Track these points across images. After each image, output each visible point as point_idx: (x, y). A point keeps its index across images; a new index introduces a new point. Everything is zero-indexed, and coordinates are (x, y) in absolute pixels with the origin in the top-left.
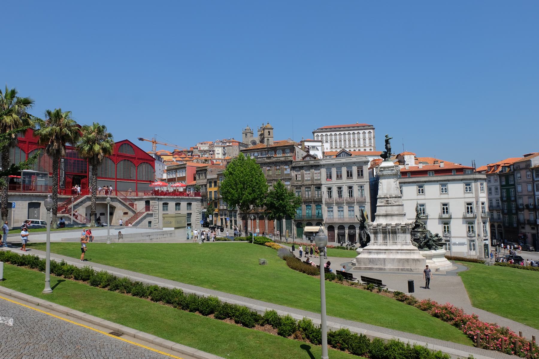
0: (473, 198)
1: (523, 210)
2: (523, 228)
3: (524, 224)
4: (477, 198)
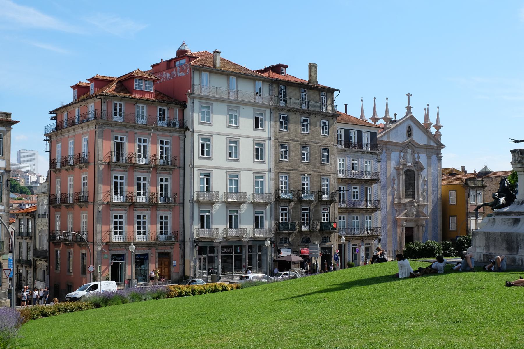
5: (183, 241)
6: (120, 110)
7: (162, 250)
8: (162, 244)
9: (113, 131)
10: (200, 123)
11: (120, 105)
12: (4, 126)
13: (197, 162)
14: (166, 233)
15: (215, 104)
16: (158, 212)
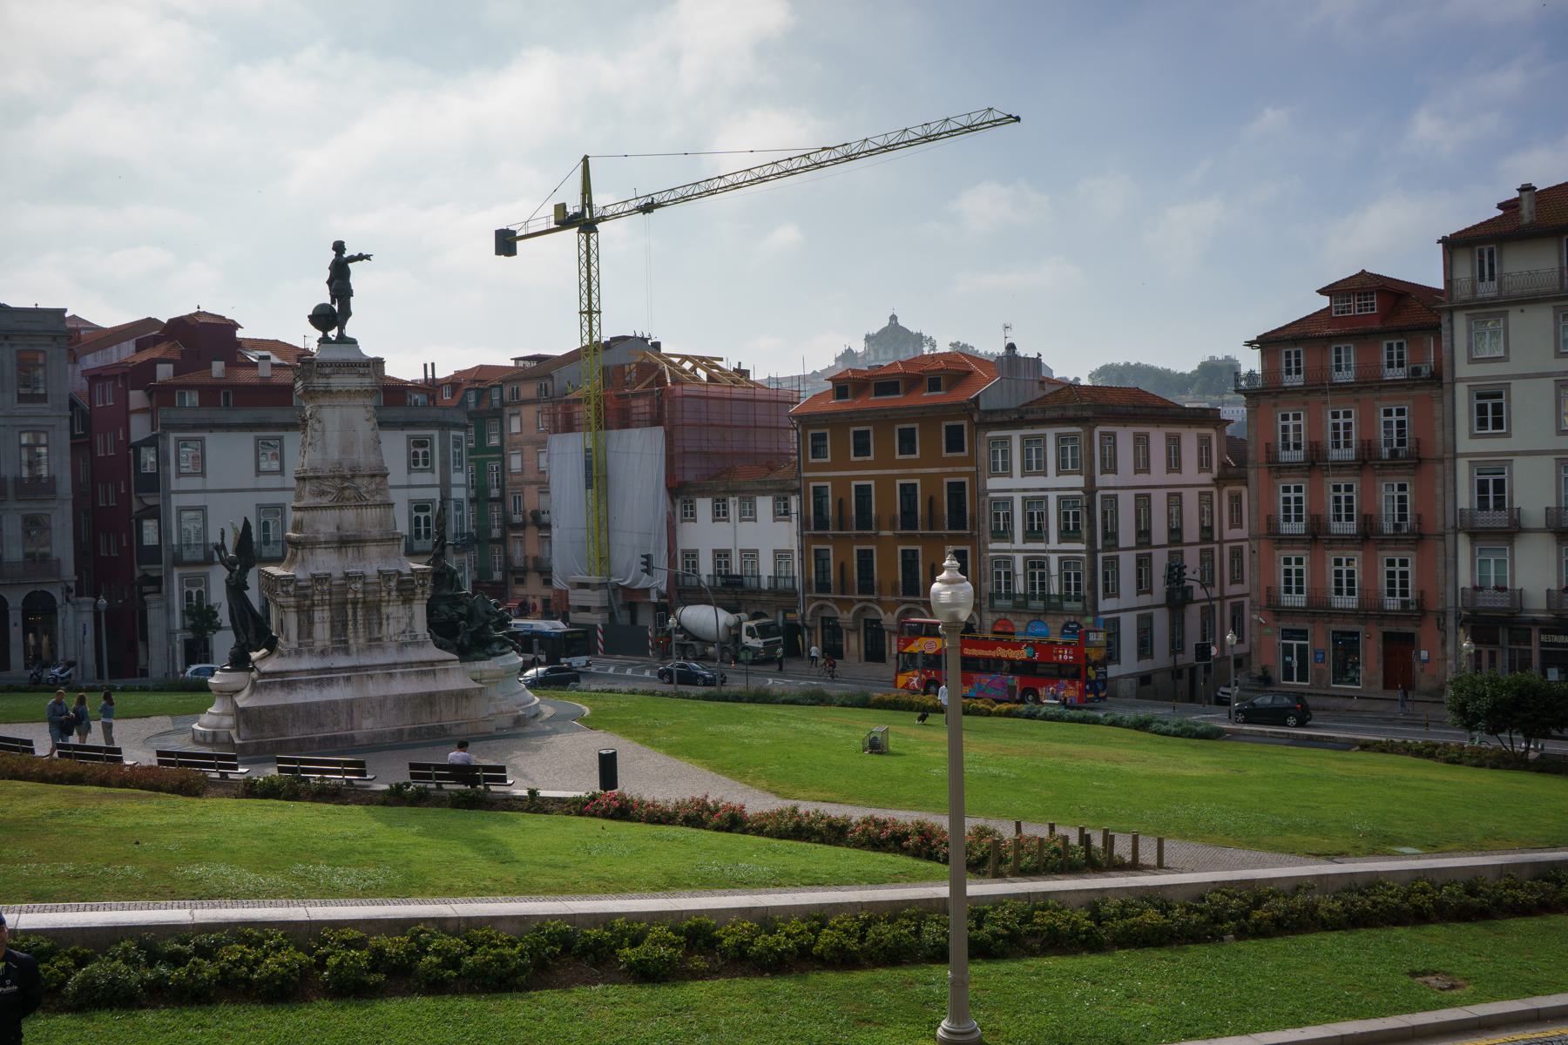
0: (434, 486)
1: (522, 526)
2: (520, 582)
3: (524, 571)
4: (445, 486)
5: (1444, 613)
6: (1298, 363)
7: (1392, 628)
8: (1394, 616)
9: (1275, 405)
10: (1472, 361)
11: (1297, 354)
13: (1465, 444)
14: (1404, 593)
16: (1380, 553)
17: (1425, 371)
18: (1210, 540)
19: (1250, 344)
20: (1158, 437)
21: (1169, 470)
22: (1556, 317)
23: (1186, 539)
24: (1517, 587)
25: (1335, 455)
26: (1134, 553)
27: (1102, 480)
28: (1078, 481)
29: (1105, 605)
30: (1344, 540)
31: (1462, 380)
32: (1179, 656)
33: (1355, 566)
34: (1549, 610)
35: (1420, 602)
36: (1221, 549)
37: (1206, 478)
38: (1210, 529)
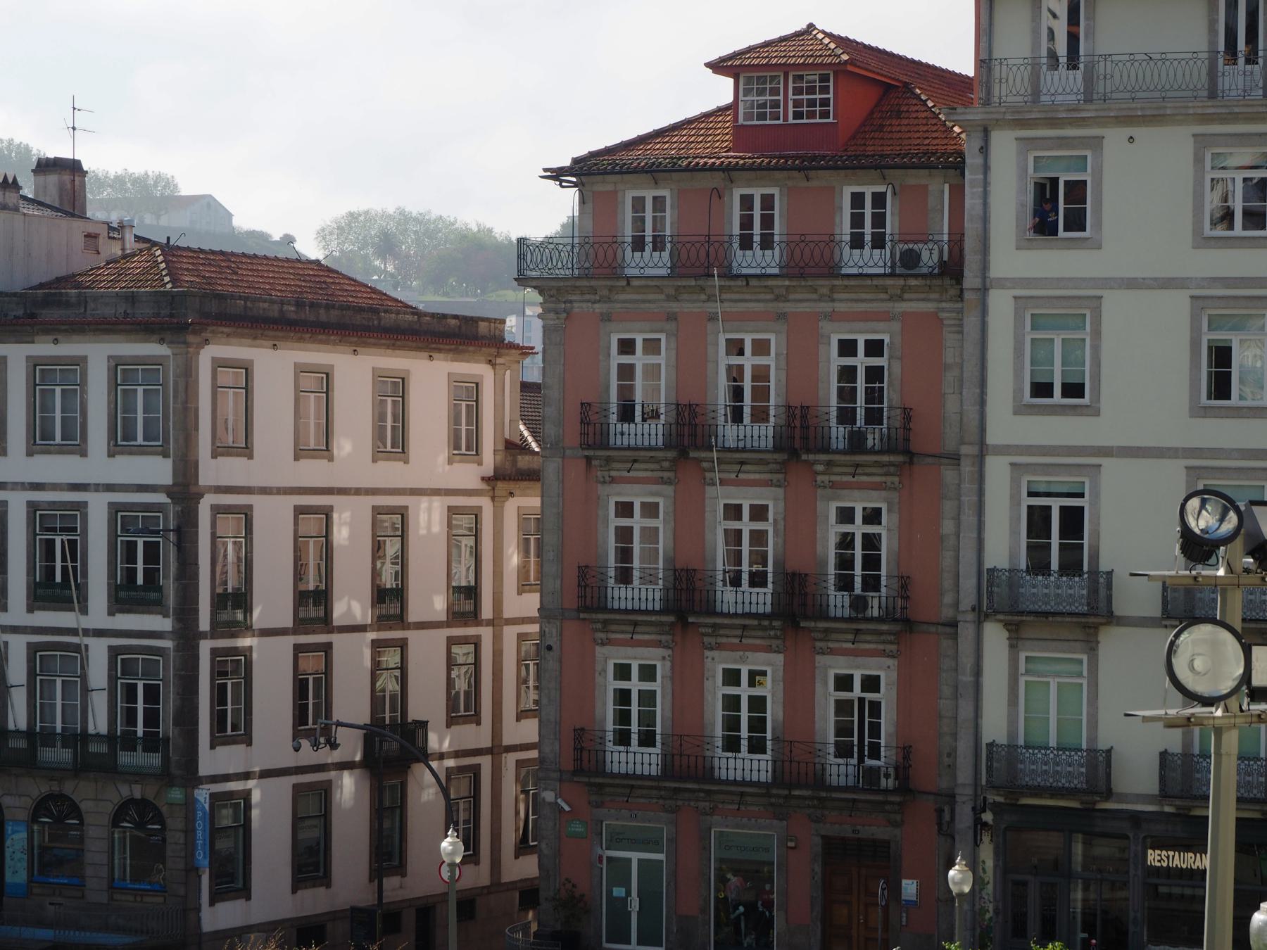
5: (951, 797)
12: (162, 341)
13: (1005, 425)
15: (1114, 137)
17: (929, 257)
18: (473, 617)
19: (557, 175)
20: (355, 371)
21: (379, 454)
22: (1198, 160)
23: (415, 613)
24: (1102, 745)
25: (730, 434)
26: (289, 642)
27: (212, 471)
28: (159, 470)
29: (212, 760)
30: (748, 626)
31: (1003, 283)
32: (390, 883)
33: (766, 689)
34: (1164, 794)
35: (902, 770)
36: (497, 639)
37: (468, 475)
38: (472, 593)
